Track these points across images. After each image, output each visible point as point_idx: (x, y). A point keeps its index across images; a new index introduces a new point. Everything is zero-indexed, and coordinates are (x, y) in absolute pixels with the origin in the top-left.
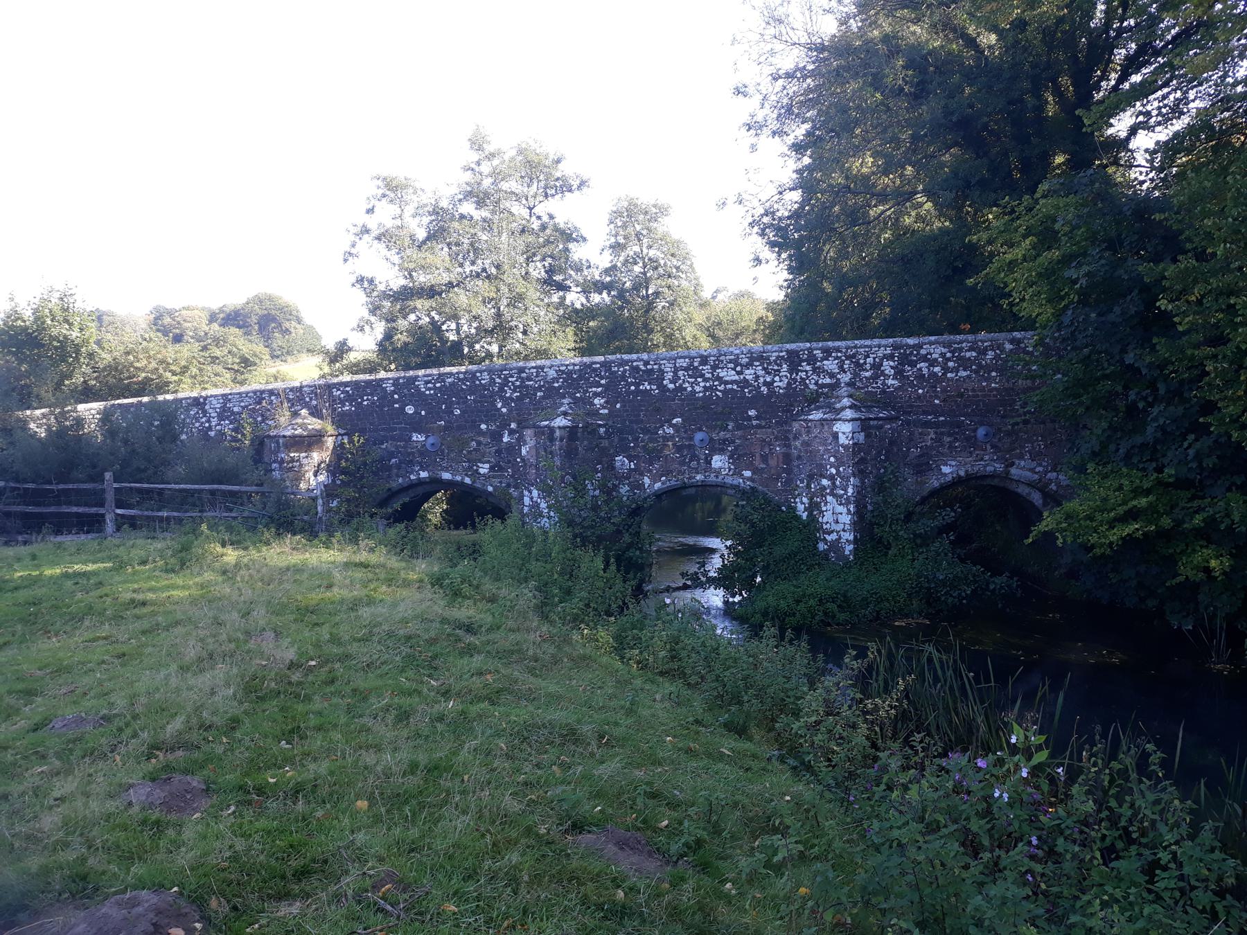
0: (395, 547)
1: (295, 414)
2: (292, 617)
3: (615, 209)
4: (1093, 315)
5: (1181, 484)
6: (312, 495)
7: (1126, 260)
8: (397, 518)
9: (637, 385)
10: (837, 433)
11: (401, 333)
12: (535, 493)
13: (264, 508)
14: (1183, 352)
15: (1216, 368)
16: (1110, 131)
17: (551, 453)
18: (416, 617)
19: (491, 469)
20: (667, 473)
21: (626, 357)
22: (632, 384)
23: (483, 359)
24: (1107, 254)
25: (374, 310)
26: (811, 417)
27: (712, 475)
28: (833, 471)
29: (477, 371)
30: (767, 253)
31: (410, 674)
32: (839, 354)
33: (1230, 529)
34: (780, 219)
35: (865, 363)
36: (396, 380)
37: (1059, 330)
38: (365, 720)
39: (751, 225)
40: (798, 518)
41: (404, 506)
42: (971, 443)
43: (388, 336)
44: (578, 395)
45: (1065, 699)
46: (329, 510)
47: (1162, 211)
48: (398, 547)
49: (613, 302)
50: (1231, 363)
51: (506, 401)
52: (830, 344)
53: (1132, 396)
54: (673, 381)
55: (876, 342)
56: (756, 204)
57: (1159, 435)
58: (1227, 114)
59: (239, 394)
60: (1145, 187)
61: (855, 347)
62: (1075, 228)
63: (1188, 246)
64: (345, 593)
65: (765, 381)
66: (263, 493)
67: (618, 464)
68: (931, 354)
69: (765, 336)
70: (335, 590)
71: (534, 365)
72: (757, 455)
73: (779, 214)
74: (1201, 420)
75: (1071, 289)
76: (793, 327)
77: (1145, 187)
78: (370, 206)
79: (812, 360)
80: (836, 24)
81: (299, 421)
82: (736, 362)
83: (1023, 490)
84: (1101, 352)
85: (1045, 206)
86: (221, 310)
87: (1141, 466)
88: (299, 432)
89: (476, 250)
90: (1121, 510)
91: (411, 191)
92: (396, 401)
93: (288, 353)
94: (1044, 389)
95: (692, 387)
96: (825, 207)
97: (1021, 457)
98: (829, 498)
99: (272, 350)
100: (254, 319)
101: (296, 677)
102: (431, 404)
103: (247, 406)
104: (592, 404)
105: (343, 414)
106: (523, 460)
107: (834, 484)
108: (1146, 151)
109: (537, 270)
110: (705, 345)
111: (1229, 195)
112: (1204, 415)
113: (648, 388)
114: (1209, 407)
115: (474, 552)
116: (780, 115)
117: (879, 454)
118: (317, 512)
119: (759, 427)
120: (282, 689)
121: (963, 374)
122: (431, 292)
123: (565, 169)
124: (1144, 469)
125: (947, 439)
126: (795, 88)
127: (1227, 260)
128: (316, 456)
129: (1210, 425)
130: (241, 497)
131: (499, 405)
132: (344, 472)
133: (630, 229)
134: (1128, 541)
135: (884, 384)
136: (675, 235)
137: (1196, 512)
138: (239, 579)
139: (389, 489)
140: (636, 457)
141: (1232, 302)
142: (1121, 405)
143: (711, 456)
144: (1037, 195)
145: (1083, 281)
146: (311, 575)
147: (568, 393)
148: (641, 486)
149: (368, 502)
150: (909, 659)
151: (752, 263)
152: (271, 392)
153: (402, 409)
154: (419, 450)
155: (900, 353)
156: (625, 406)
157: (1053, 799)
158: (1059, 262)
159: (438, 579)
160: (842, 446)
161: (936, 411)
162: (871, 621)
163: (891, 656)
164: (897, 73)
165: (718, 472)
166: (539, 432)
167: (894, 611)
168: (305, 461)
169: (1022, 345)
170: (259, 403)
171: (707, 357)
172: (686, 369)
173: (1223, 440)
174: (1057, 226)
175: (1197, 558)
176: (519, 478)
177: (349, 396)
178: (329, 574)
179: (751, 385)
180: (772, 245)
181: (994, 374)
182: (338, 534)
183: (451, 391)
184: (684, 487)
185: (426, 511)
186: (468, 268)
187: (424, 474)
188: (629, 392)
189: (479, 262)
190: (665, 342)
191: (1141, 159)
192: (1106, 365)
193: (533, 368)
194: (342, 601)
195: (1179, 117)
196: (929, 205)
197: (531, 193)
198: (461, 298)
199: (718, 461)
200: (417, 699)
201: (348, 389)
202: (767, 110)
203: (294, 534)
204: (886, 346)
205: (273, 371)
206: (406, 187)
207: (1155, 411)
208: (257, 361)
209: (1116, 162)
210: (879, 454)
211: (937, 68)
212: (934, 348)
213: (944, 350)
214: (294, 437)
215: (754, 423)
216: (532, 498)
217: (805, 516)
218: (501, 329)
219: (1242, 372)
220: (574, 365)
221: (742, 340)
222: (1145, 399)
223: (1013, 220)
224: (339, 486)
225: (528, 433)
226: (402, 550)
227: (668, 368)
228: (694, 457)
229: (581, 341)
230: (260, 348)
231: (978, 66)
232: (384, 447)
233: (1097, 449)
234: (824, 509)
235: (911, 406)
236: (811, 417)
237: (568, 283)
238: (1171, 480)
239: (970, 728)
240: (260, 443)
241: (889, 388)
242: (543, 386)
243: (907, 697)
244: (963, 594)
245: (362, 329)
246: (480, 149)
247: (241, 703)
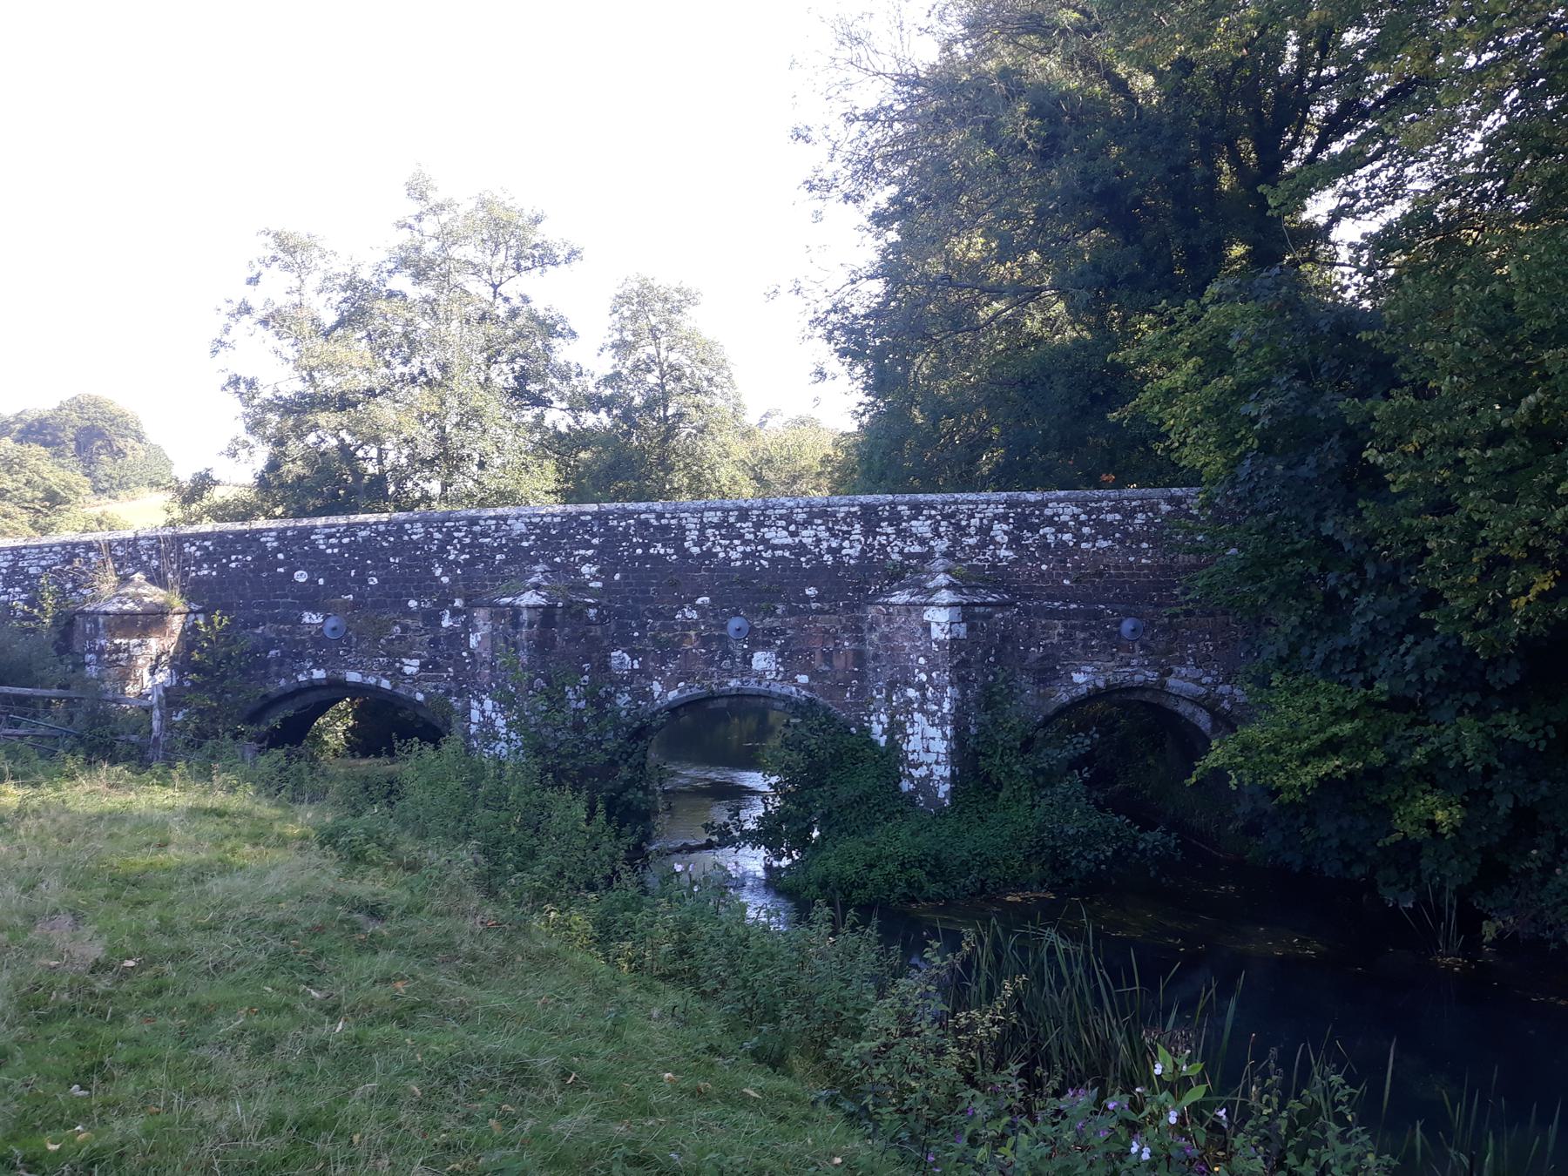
0: (269, 784)
1: (125, 580)
2: (103, 892)
3: (620, 292)
4: (1279, 467)
5: (1397, 703)
6: (145, 703)
7: (1323, 392)
8: (275, 740)
9: (646, 547)
10: (929, 623)
11: (293, 461)
12: (488, 704)
13: (69, 723)
14: (1397, 521)
15: (1440, 545)
16: (1305, 216)
17: (514, 644)
18: (291, 895)
19: (423, 666)
20: (686, 676)
21: (630, 506)
22: (639, 545)
23: (417, 503)
24: (1297, 384)
26: (893, 600)
27: (753, 680)
28: (924, 677)
29: (405, 522)
30: (834, 365)
31: (280, 980)
32: (933, 512)
33: (1462, 768)
34: (855, 317)
35: (968, 526)
36: (281, 534)
37: (1233, 487)
38: (204, 1052)
39: (816, 322)
40: (873, 744)
41: (284, 721)
42: (1113, 641)
43: (274, 466)
44: (558, 560)
45: (1238, 1005)
46: (169, 727)
47: (1370, 328)
48: (271, 786)
49: (616, 426)
50: (1460, 539)
51: (449, 567)
52: (920, 497)
53: (1332, 582)
55: (983, 496)
56: (820, 295)
57: (1367, 635)
58: (1455, 203)
59: (39, 547)
60: (1351, 292)
61: (955, 502)
62: (1256, 346)
63: (1404, 377)
64: (190, 857)
65: (829, 546)
66: (70, 700)
67: (615, 662)
68: (1059, 516)
69: (833, 481)
70: (172, 850)
72: (817, 652)
73: (853, 311)
74: (1422, 616)
75: (1249, 430)
76: (869, 469)
77: (1351, 292)
78: (253, 275)
79: (896, 518)
80: (937, 48)
81: (130, 590)
82: (789, 519)
83: (1184, 709)
84: (1289, 520)
85: (1215, 316)
86: (18, 418)
87: (1344, 678)
88: (129, 606)
89: (411, 343)
90: (1317, 739)
91: (316, 253)
92: (281, 563)
93: (120, 485)
94: (1213, 569)
95: (725, 551)
96: (916, 304)
97: (1182, 662)
98: (917, 716)
99: (96, 481)
100: (70, 433)
101: (102, 985)
102: (333, 568)
103: (50, 567)
104: (578, 573)
105: (199, 581)
106: (471, 654)
107: (924, 695)
108: (1351, 245)
109: (503, 376)
110: (747, 491)
111: (1457, 311)
112: (1427, 610)
113: (662, 551)
114: (1432, 599)
115: (391, 792)
116: (856, 172)
117: (987, 654)
118: (151, 731)
119: (819, 611)
120: (79, 1004)
122: (343, 402)
123: (546, 233)
124: (1348, 683)
126: (879, 136)
127: (1455, 398)
128: (154, 644)
129: (1434, 622)
130: (34, 705)
131: (438, 572)
132: (197, 668)
133: (642, 323)
134: (1326, 783)
135: (994, 555)
136: (708, 334)
137: (1418, 744)
138: (22, 832)
139: (265, 696)
140: (643, 652)
141: (1460, 455)
142: (1318, 593)
143: (751, 652)
144: (1205, 300)
145: (1265, 420)
146: (137, 828)
147: (542, 556)
149: (231, 715)
150: (1023, 951)
151: (813, 378)
152: (89, 546)
153: (289, 574)
154: (312, 638)
157: (1221, 1154)
158: (1233, 393)
159: (331, 836)
160: (935, 641)
162: (973, 895)
163: (997, 946)
164: (1019, 122)
165: (761, 676)
166: (498, 613)
167: (1005, 880)
168: (137, 651)
169: (1184, 506)
170: (70, 562)
171: (747, 510)
172: (717, 526)
173: (1451, 643)
174: (1231, 344)
175: (1419, 808)
176: (464, 682)
178: (164, 825)
179: (810, 552)
180: (843, 353)
181: (1145, 545)
182: (181, 765)
183: (365, 550)
184: (712, 697)
185: (320, 729)
186: (400, 369)
187: (318, 674)
188: (633, 558)
189: (416, 361)
190: (690, 485)
191: (1344, 255)
192: (1296, 537)
193: (491, 518)
194: (180, 870)
195: (1392, 203)
196: (1060, 307)
197: (497, 265)
198: (385, 412)
200: (288, 1019)
201: (207, 543)
202: (838, 164)
203: (114, 763)
204: (997, 503)
205: (96, 512)
206: (306, 248)
207: (1362, 601)
208: (72, 497)
209: (1312, 258)
210: (987, 654)
211: (1073, 117)
212: (1063, 506)
213: (1077, 511)
214: (122, 614)
215: (814, 605)
216: (483, 712)
217: (883, 741)
218: (447, 459)
219: (1474, 551)
220: (553, 515)
221: (802, 486)
222: (1348, 584)
223: (1172, 333)
224: (189, 690)
225: (481, 614)
226: (279, 790)
227: (691, 523)
228: (727, 653)
229: (566, 481)
230: (76, 477)
231: (1128, 119)
232: (259, 631)
233: (1285, 653)
234: (910, 731)
235: (1031, 588)
236: (893, 600)
237: (548, 395)
238: (1384, 698)
239: (1107, 1051)
240: (69, 625)
241: (1001, 561)
242: (506, 545)
243: (1019, 1007)
244: (1102, 857)
246: (422, 197)
247: (11, 1025)
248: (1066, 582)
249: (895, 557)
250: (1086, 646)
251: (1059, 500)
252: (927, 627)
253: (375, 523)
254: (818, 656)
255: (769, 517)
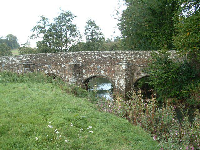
92: (43, 59)
131: (62, 60)
166: (69, 65)
199: (102, 72)
251: (140, 52)
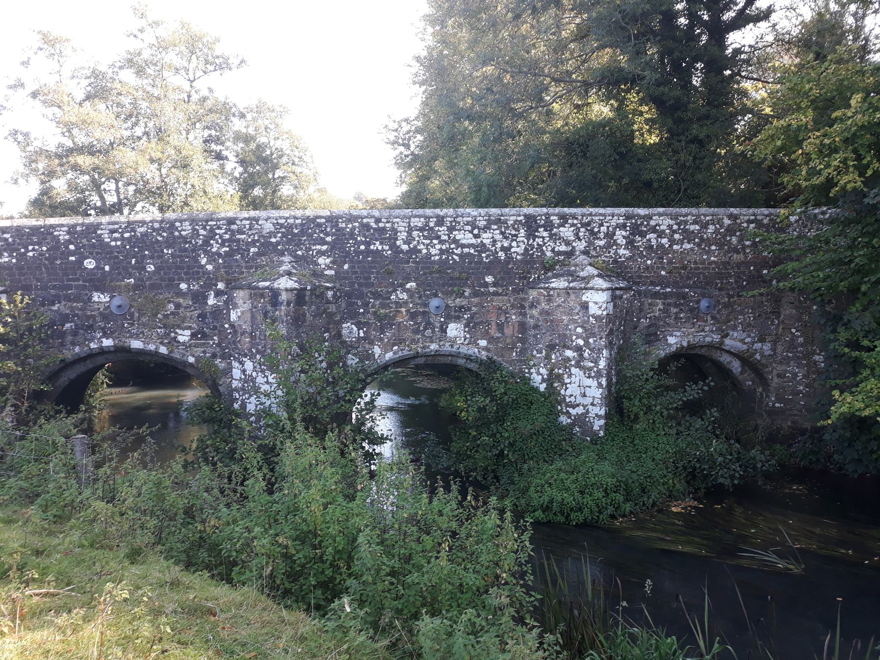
9: (368, 244)
10: (587, 303)
12: (249, 365)
19: (193, 335)
20: (400, 341)
22: (362, 243)
25: (31, 161)
27: (447, 344)
28: (581, 342)
29: (176, 220)
32: (575, 221)
35: (599, 232)
40: (536, 390)
42: (695, 314)
54: (407, 242)
55: (609, 210)
61: (591, 215)
65: (502, 245)
67: (345, 332)
71: (247, 216)
72: (493, 323)
79: (548, 226)
82: (473, 225)
83: (725, 358)
92: (72, 253)
95: (427, 249)
97: (734, 328)
102: (117, 257)
106: (232, 326)
113: (380, 248)
119: (496, 294)
121: (687, 246)
125: (674, 310)
131: (204, 261)
135: (616, 253)
140: (366, 324)
148: (370, 356)
153: (80, 262)
154: (101, 314)
155: (632, 224)
156: (353, 267)
160: (593, 316)
161: (663, 282)
165: (453, 342)
166: (256, 294)
171: (443, 217)
172: (421, 230)
176: (227, 347)
177: (9, 244)
179: (488, 250)
181: (713, 248)
184: (417, 356)
187: (107, 343)
188: (358, 252)
193: (245, 219)
199: (454, 330)
201: (7, 236)
204: (619, 215)
213: (672, 222)
215: (492, 289)
216: (244, 371)
217: (542, 387)
220: (295, 218)
225: (240, 296)
227: (402, 227)
228: (429, 325)
232: (55, 308)
234: (567, 381)
235: (640, 277)
236: (552, 285)
241: (620, 257)
242: (258, 241)
245: (16, 182)
248: (663, 273)
249: (549, 254)
250: (677, 318)
251: (660, 215)
252: (585, 306)
253: (151, 222)
254: (494, 327)
255: (459, 223)
